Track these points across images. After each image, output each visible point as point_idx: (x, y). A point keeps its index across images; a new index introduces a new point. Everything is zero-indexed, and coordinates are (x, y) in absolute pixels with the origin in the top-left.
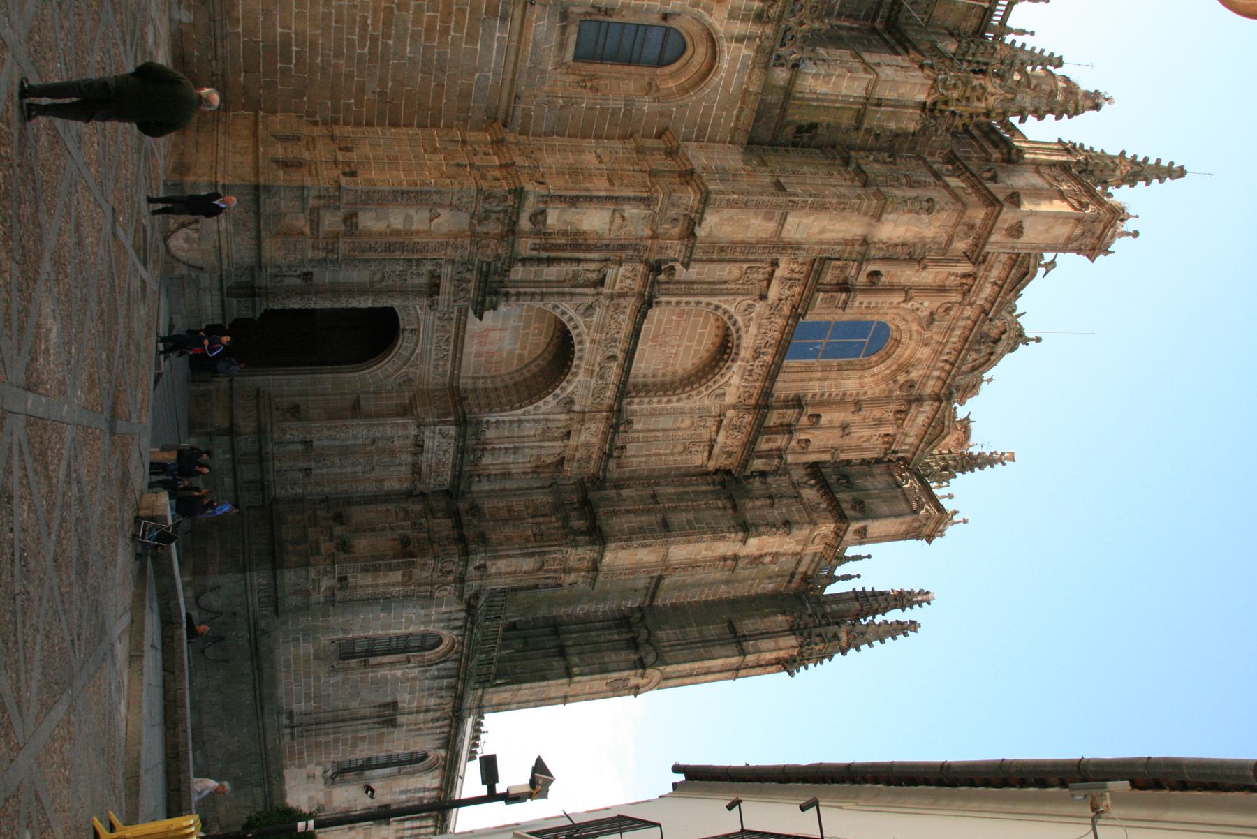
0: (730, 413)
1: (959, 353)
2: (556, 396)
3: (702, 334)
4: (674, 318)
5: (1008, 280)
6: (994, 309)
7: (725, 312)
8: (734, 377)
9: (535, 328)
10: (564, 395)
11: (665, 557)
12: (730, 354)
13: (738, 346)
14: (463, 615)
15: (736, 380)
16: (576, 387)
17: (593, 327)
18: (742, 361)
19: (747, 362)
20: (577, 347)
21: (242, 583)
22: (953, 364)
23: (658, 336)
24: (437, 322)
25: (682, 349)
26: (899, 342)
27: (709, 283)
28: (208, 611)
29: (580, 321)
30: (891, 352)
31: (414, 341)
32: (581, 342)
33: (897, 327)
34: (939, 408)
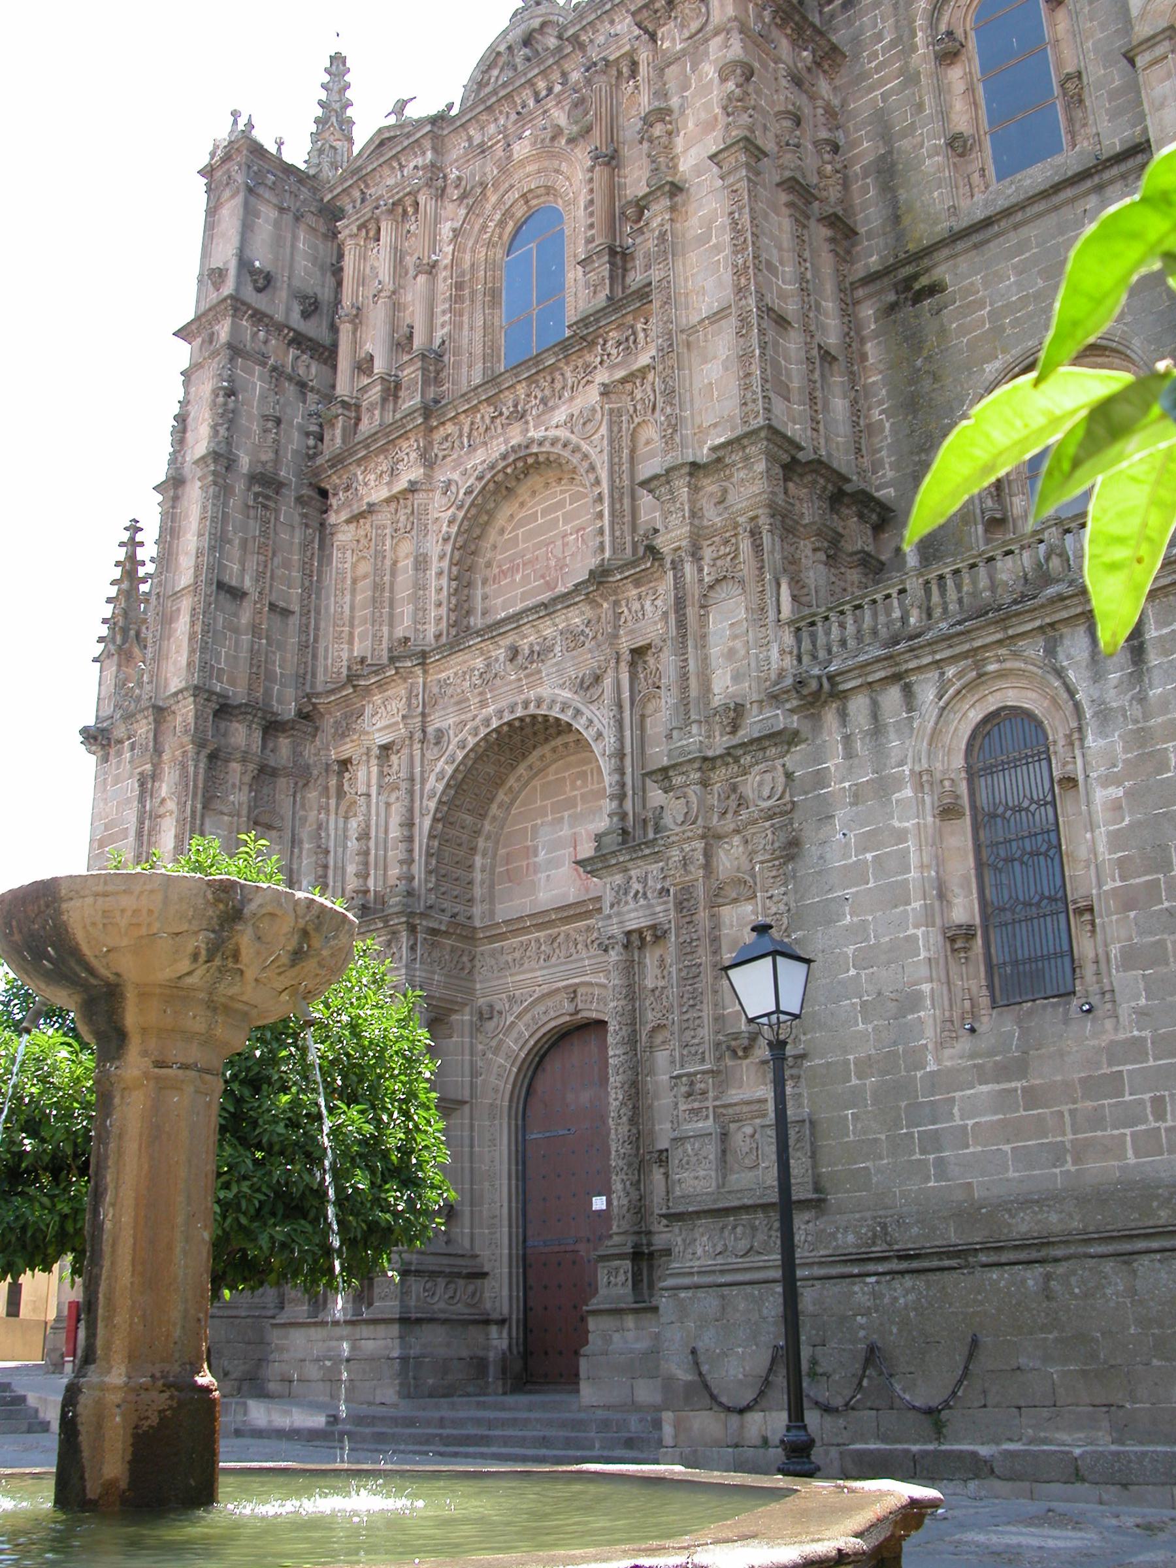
0: (602, 376)
1: (509, 96)
2: (578, 712)
3: (545, 512)
4: (518, 578)
5: (382, 160)
6: (419, 135)
7: (451, 522)
8: (554, 422)
9: (574, 788)
10: (576, 700)
11: (717, 317)
12: (524, 458)
13: (504, 457)
14: (859, 705)
15: (560, 415)
16: (562, 686)
17: (463, 717)
18: (527, 430)
19: (527, 423)
20: (495, 724)
21: (683, 1295)
22: (530, 83)
23: (547, 583)
24: (554, 960)
25: (568, 528)
26: (524, 195)
27: (392, 584)
28: (767, 1382)
29: (455, 741)
30: (542, 190)
31: (590, 990)
32: (487, 721)
33: (502, 223)
34: (583, 28)
